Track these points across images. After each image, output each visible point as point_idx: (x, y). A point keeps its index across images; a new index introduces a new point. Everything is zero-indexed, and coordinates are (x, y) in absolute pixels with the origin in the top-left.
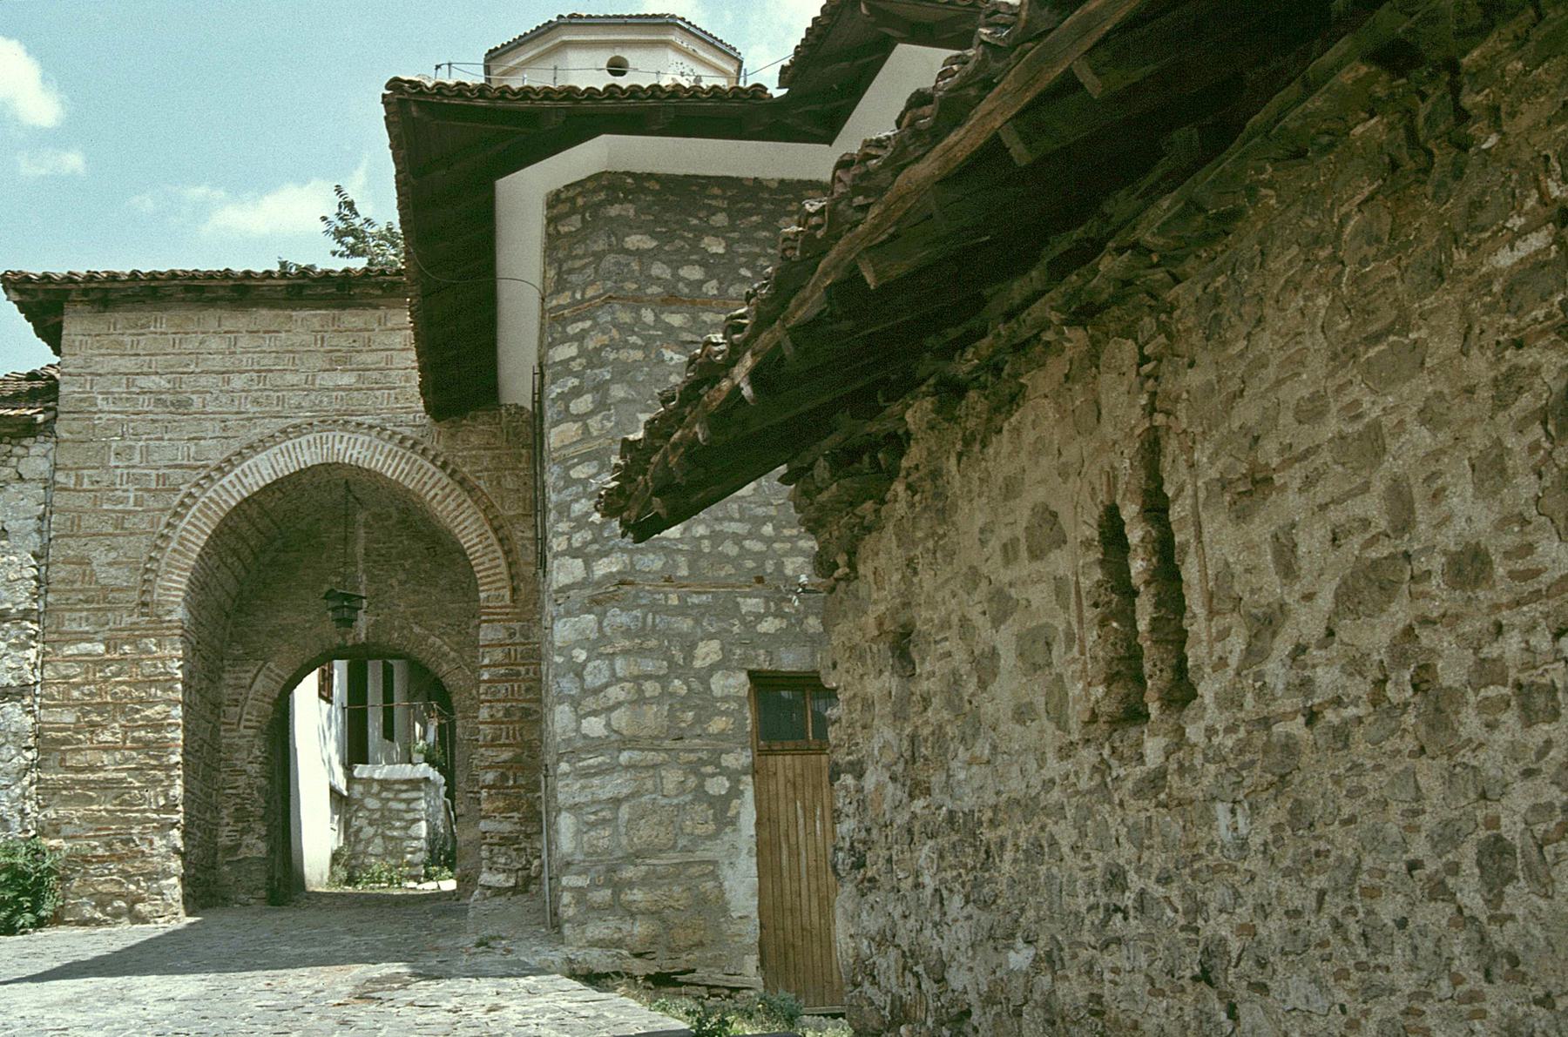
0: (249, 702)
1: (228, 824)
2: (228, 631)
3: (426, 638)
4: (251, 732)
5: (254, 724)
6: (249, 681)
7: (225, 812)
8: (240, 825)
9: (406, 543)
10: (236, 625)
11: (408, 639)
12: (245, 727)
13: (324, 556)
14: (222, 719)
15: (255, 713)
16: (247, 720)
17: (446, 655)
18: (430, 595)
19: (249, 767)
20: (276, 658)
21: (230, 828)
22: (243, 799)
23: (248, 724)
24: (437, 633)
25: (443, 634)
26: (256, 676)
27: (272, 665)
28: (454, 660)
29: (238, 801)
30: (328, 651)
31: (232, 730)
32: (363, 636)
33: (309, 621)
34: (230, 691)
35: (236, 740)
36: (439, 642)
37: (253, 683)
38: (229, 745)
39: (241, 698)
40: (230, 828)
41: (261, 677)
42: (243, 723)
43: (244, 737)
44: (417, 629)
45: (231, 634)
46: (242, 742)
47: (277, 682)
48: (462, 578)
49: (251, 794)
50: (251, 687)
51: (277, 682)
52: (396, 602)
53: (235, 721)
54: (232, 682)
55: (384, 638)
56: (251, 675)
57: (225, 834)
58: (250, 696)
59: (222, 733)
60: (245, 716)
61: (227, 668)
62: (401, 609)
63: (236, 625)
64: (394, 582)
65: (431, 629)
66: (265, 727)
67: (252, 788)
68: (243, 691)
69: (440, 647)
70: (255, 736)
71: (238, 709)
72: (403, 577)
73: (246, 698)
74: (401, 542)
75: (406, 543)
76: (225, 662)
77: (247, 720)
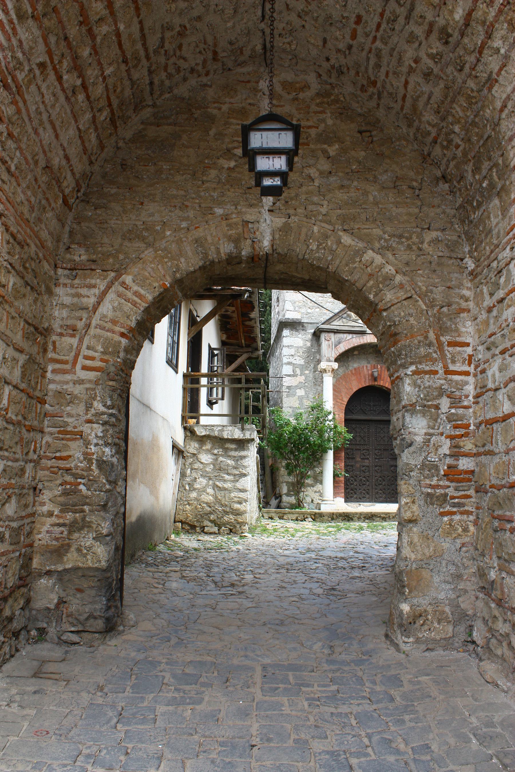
0: (92, 331)
1: (50, 514)
2: (67, 229)
3: (360, 253)
4: (92, 375)
5: (98, 364)
6: (92, 300)
7: (46, 496)
8: (70, 516)
9: (330, 122)
10: (79, 220)
11: (332, 251)
12: (85, 368)
13: (212, 133)
14: (51, 355)
15: (100, 348)
16: (86, 358)
17: (389, 278)
18: (366, 193)
19: (86, 428)
20: (135, 270)
21: (54, 520)
22: (76, 476)
23: (88, 363)
24: (377, 245)
25: (388, 248)
26: (104, 293)
27: (128, 279)
28: (401, 286)
29: (69, 478)
30: (212, 262)
31: (64, 372)
32: (266, 243)
33: (186, 219)
34: (65, 313)
35: (69, 387)
36: (378, 260)
37: (99, 303)
38: (59, 393)
39: (80, 325)
40: (54, 520)
41: (111, 295)
42: (81, 361)
43: (81, 382)
44: (347, 239)
45: (71, 233)
46: (78, 390)
47: (134, 304)
48: (411, 174)
49: (90, 469)
50: (95, 309)
51: (134, 304)
52: (315, 199)
53: (70, 358)
54: (67, 300)
55: (299, 249)
56: (96, 291)
57: (45, 528)
58: (94, 323)
59: (49, 375)
60: (85, 352)
61: (62, 280)
62: (324, 210)
63: (79, 220)
64: (313, 172)
65: (368, 240)
66: (113, 369)
67: (90, 461)
68: (85, 315)
69: (381, 267)
70: (97, 383)
71: (74, 341)
72: (324, 165)
73: (88, 326)
74: (324, 121)
75: (330, 122)
76: (60, 271)
77: (86, 358)
